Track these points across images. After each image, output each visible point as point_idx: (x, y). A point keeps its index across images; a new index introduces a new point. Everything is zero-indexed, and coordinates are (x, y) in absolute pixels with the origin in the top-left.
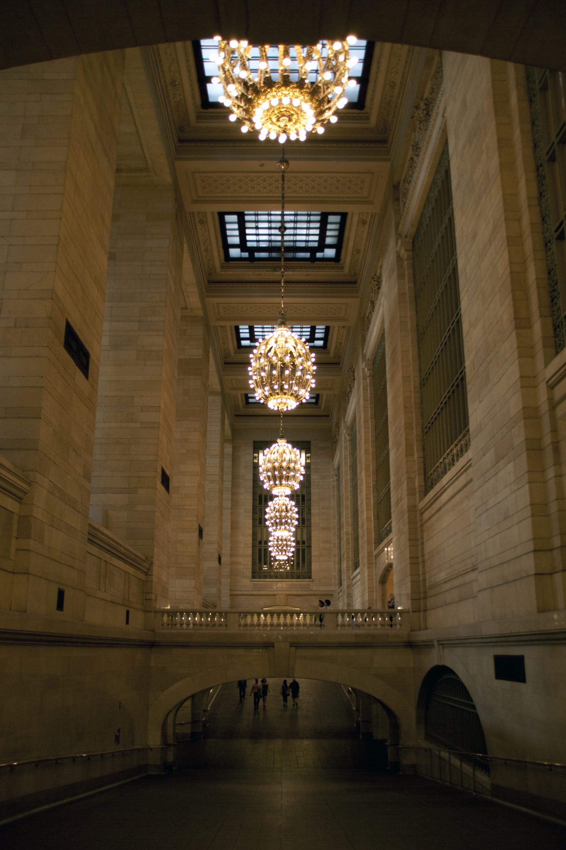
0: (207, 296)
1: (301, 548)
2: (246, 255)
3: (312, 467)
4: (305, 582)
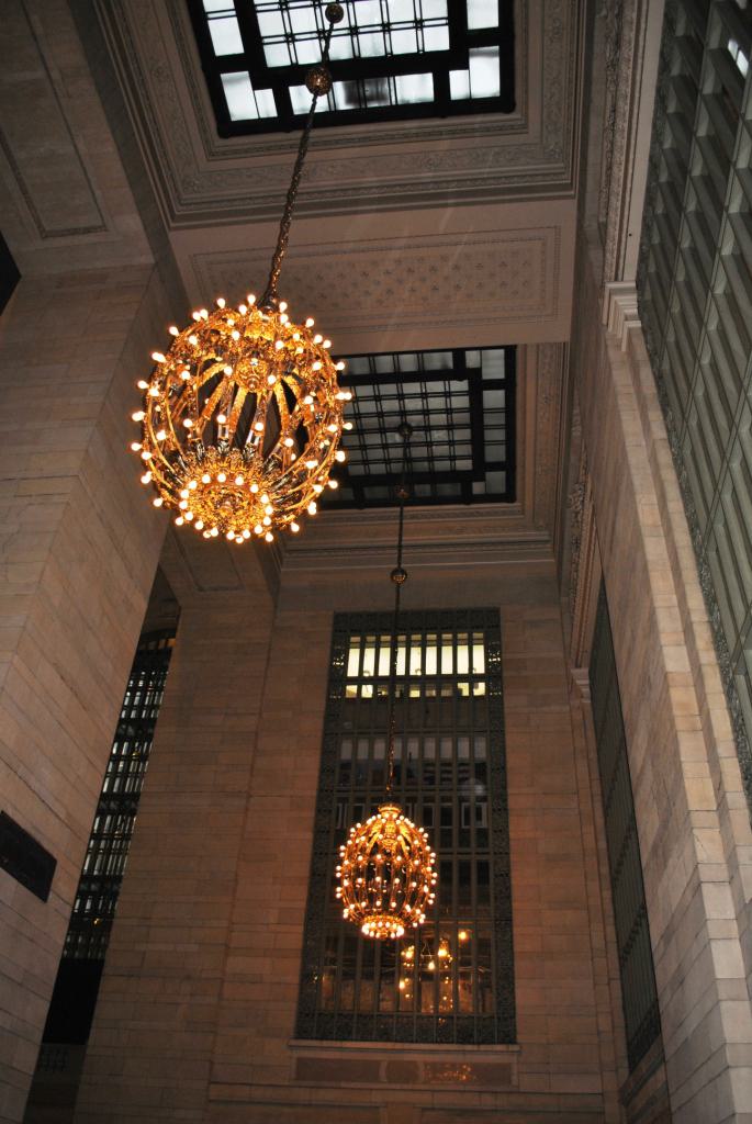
1: (455, 859)
3: (505, 674)
4: (493, 1054)
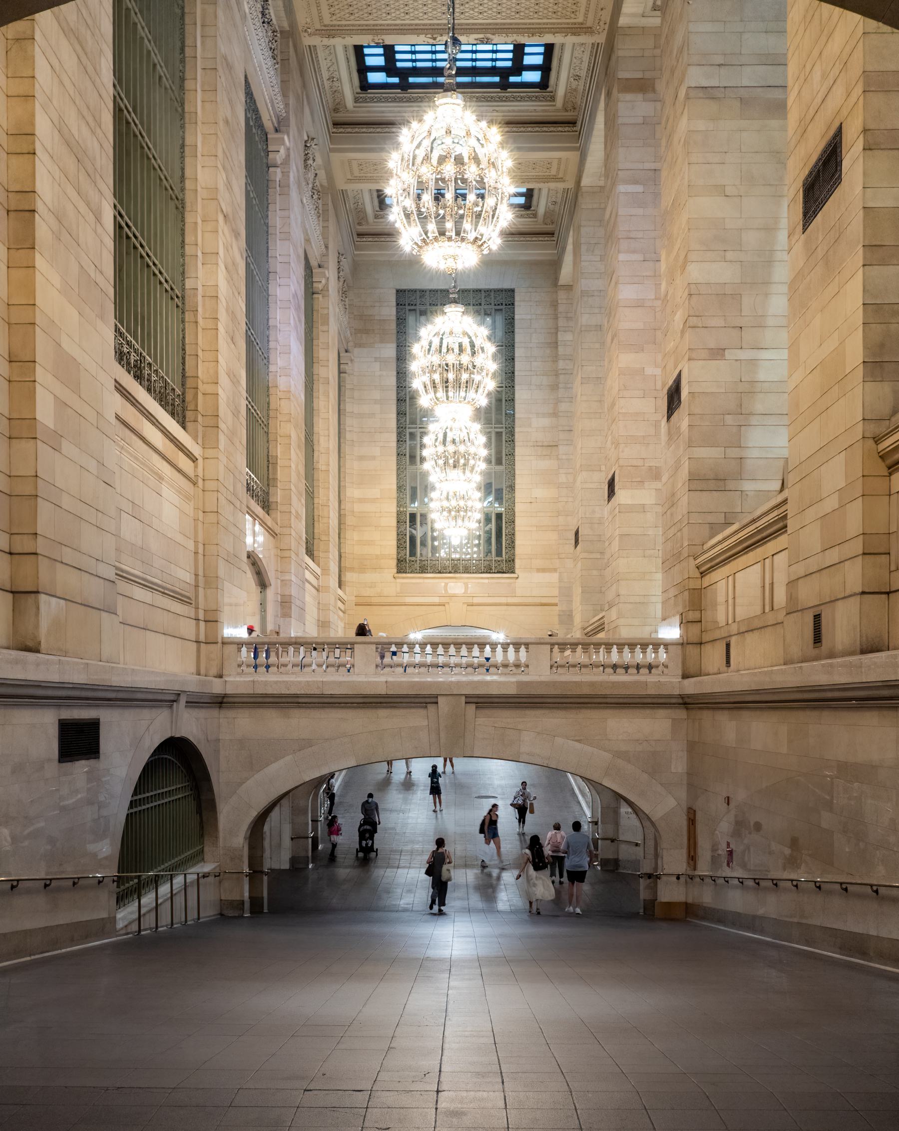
0: (332, 150)
2: (396, 80)
